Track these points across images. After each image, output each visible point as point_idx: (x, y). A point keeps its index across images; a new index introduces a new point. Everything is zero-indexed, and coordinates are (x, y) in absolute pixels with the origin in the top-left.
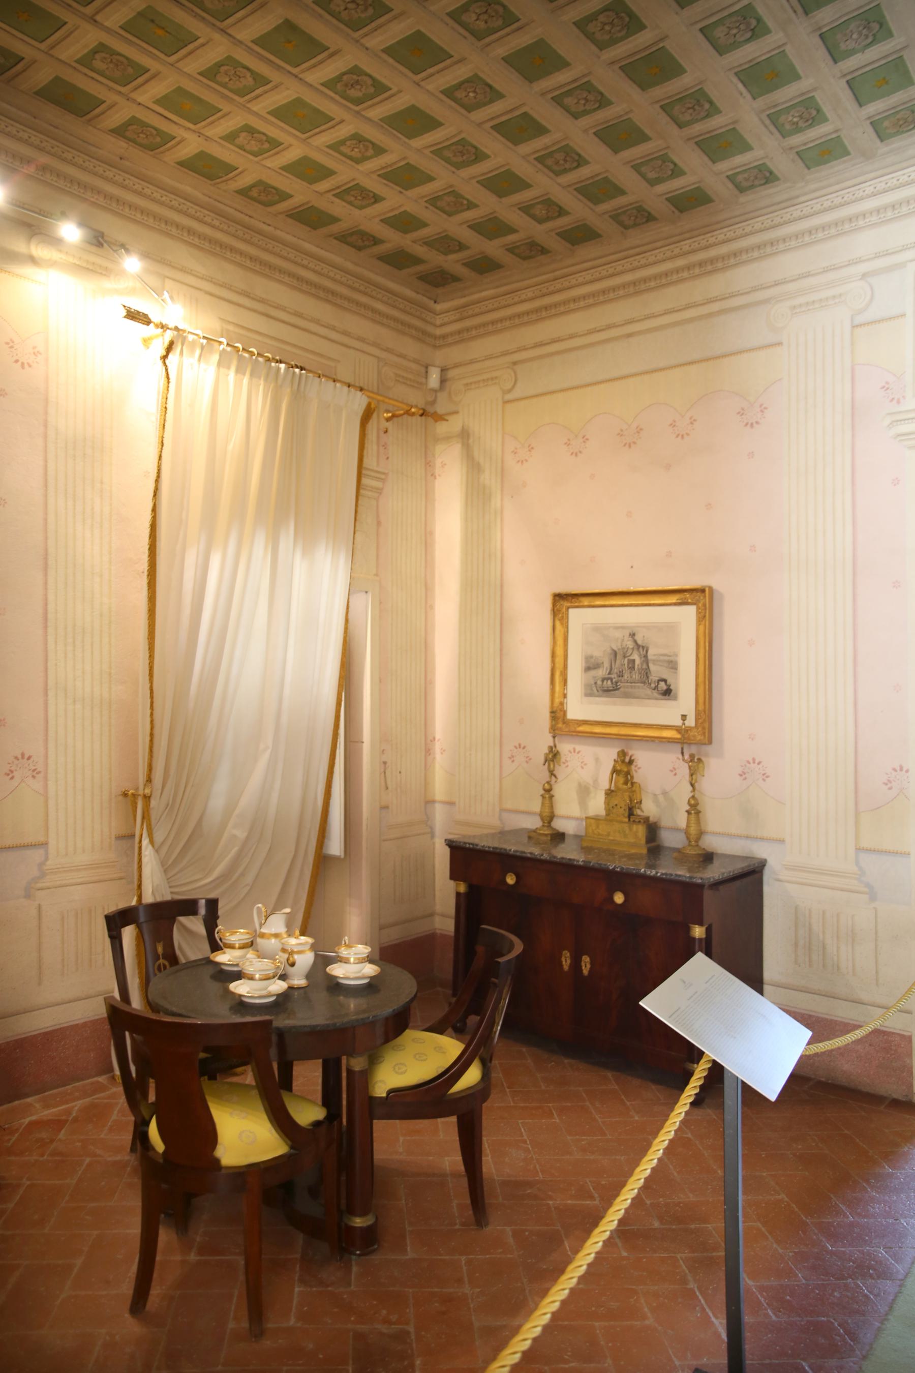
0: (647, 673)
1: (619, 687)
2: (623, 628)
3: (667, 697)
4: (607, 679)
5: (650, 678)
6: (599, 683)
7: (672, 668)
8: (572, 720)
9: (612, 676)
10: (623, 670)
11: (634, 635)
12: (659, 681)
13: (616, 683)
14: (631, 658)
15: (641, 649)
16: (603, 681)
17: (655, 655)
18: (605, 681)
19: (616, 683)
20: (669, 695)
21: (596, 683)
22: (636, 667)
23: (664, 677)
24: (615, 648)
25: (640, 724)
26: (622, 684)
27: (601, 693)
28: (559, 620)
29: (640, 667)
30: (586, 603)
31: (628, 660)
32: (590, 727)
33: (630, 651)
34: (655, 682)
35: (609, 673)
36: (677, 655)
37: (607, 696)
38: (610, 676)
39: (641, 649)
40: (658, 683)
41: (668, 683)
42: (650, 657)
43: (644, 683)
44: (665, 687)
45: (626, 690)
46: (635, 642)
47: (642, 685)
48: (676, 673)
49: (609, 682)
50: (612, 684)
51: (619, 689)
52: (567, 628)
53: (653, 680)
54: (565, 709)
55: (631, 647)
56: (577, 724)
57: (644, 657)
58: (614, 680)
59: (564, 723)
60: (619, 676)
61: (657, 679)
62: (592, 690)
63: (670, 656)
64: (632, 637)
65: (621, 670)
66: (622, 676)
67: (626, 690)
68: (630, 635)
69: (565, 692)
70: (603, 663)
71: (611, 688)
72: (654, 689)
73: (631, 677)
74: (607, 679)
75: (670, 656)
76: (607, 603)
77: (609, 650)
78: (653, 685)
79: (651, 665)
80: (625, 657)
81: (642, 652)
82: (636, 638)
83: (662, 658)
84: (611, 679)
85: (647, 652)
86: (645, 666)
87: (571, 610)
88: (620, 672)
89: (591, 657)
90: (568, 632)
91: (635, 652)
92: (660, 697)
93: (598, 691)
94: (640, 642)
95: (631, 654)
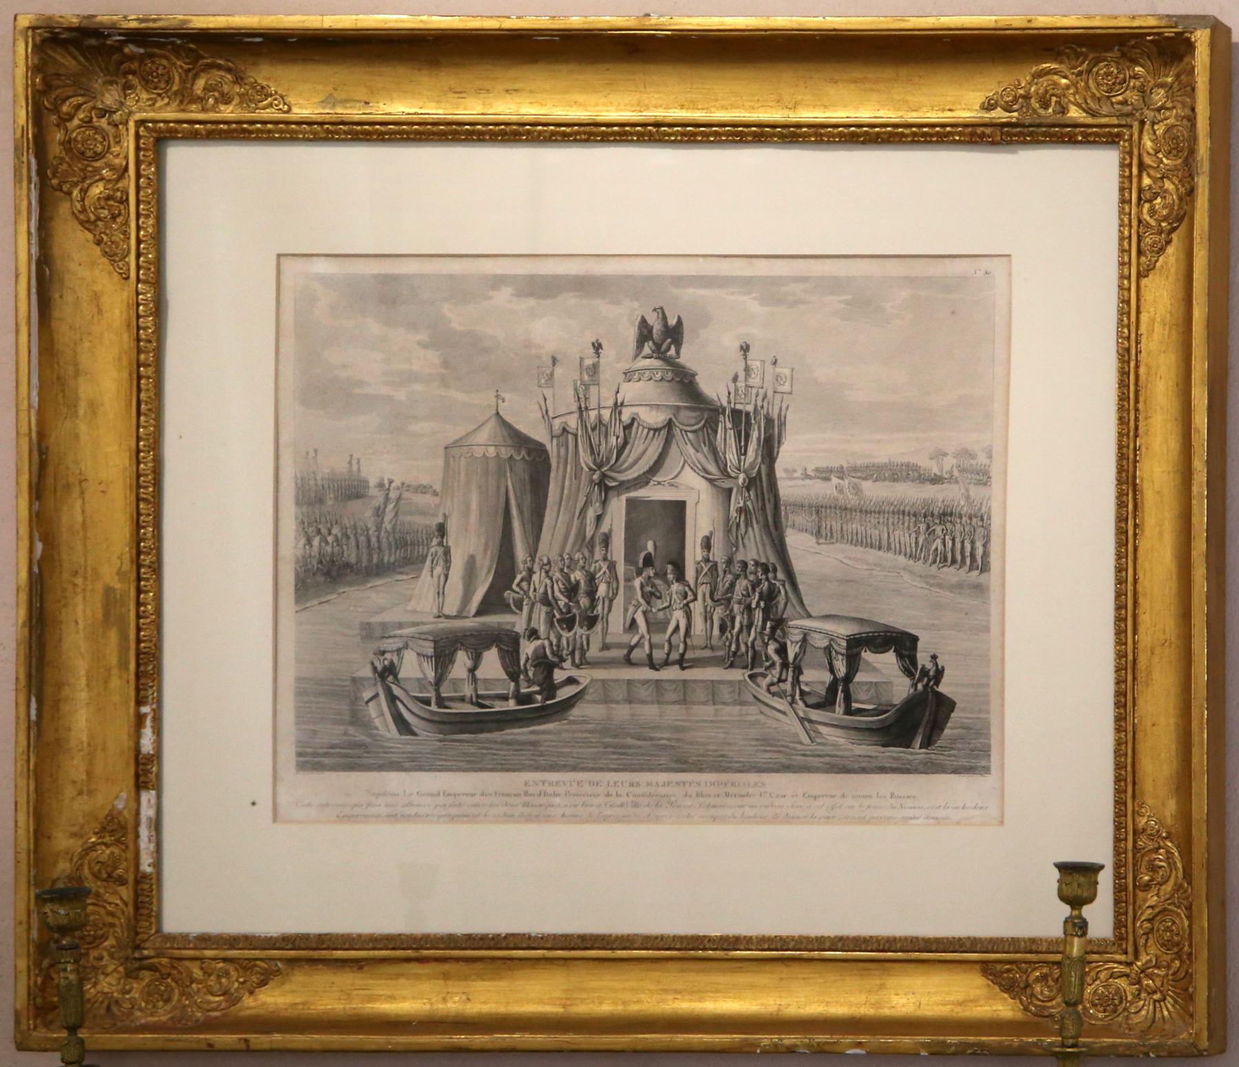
0: (770, 597)
1: (564, 693)
2: (587, 286)
3: (917, 752)
4: (478, 643)
5: (797, 625)
6: (414, 667)
7: (946, 560)
8: (205, 940)
9: (518, 623)
10: (591, 578)
11: (674, 334)
12: (856, 645)
13: (546, 665)
14: (655, 493)
15: (725, 436)
16: (443, 652)
17: (824, 474)
18: (462, 659)
19: (546, 665)
20: (928, 743)
21: (388, 673)
22: (693, 554)
23: (899, 617)
24: (539, 434)
25: (734, 942)
26: (585, 676)
27: (426, 736)
28: (87, 225)
29: (718, 554)
30: (304, 109)
31: (631, 503)
32: (346, 979)
33: (643, 451)
34: (828, 650)
35: (492, 603)
36: (983, 477)
37: (473, 765)
38: (492, 620)
39: (725, 436)
40: (853, 662)
41: (923, 659)
42: (786, 489)
43: (752, 660)
44: (901, 688)
45: (622, 712)
46: (685, 383)
47: (737, 675)
48: (980, 590)
49: (492, 663)
50: (514, 676)
51: (570, 703)
52: (157, 281)
53: (820, 642)
54: (146, 866)
55: (655, 418)
56: (246, 966)
57: (752, 483)
58: (528, 648)
59: (135, 967)
60: (569, 623)
61: (844, 630)
62: (357, 719)
63: (936, 480)
64: (659, 353)
65: (577, 576)
66: (591, 622)
67: (622, 712)
68: (645, 332)
69: (147, 744)
70: (442, 530)
71: (512, 705)
72: (826, 703)
73: (656, 626)
74: (478, 643)
75: (936, 480)
76: (472, 109)
77: (486, 442)
78: (816, 677)
79: (797, 541)
80: (605, 488)
81: (731, 457)
82: (688, 356)
83: (874, 491)
84: (508, 644)
85: (769, 450)
86: (754, 548)
87: (179, 157)
88: (572, 591)
89: (353, 490)
90: (159, 308)
91: (685, 450)
92: (866, 749)
93: (403, 725)
94: (714, 388)
95: (655, 468)
